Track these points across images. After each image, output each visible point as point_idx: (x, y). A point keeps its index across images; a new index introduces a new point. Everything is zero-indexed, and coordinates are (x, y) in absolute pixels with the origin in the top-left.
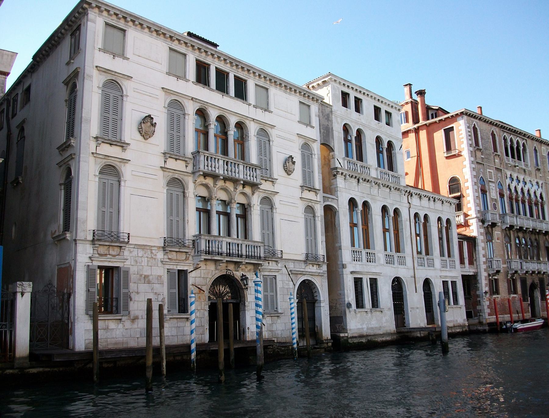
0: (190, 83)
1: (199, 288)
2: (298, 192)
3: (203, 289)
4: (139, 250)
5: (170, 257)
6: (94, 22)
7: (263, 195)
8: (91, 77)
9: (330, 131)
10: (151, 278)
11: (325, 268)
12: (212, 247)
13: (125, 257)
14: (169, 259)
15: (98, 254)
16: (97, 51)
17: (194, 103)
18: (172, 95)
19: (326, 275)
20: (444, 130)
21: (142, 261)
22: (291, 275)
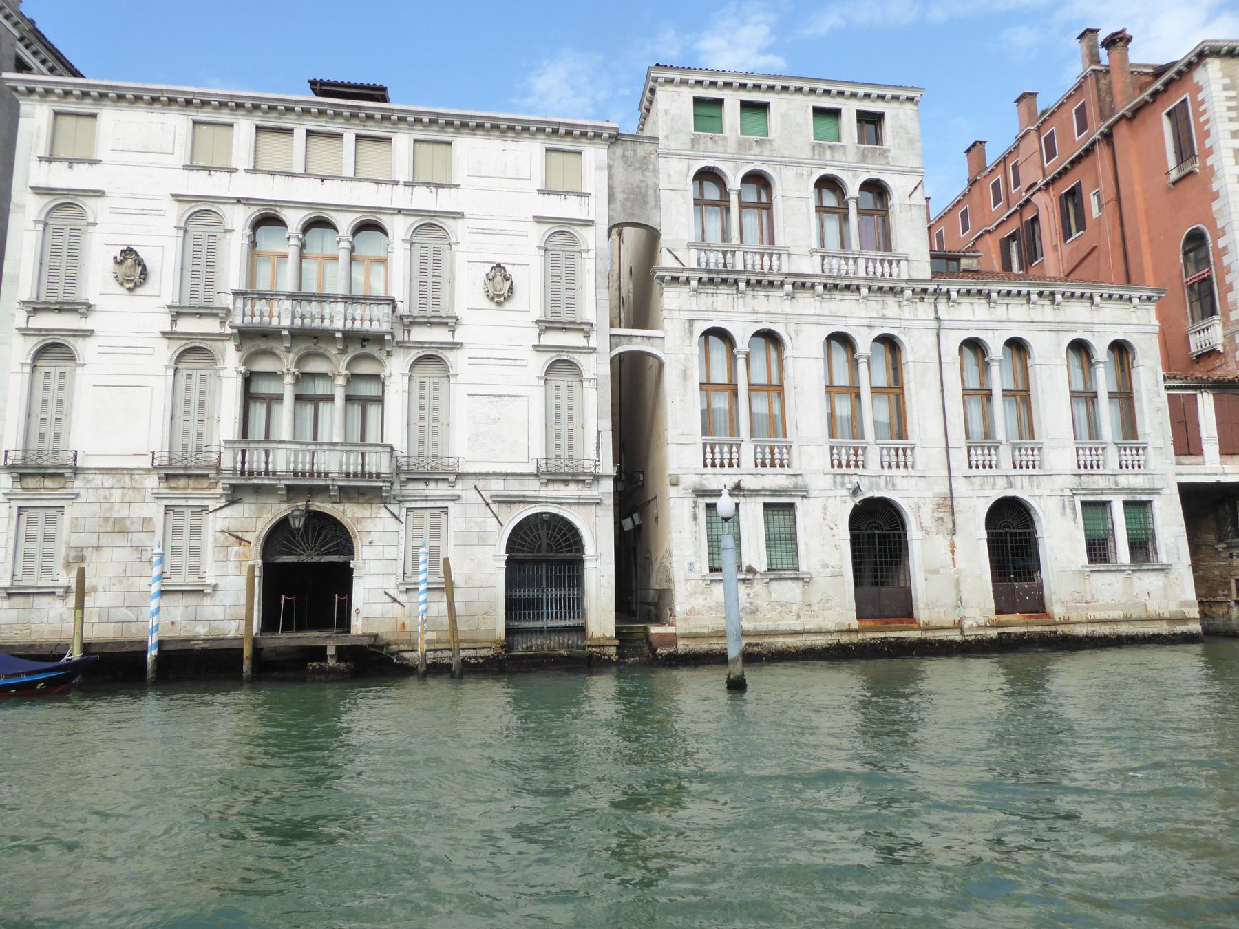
0: (241, 173)
1: (237, 537)
2: (532, 336)
3: (246, 538)
4: (108, 477)
5: (173, 485)
6: (30, 116)
7: (414, 354)
8: (22, 207)
9: (651, 192)
10: (128, 522)
11: (607, 487)
12: (251, 462)
13: (76, 491)
14: (170, 488)
15: (23, 488)
16: (35, 164)
17: (246, 207)
18: (194, 204)
19: (609, 501)
20: (1169, 114)
21: (111, 495)
22: (493, 506)
